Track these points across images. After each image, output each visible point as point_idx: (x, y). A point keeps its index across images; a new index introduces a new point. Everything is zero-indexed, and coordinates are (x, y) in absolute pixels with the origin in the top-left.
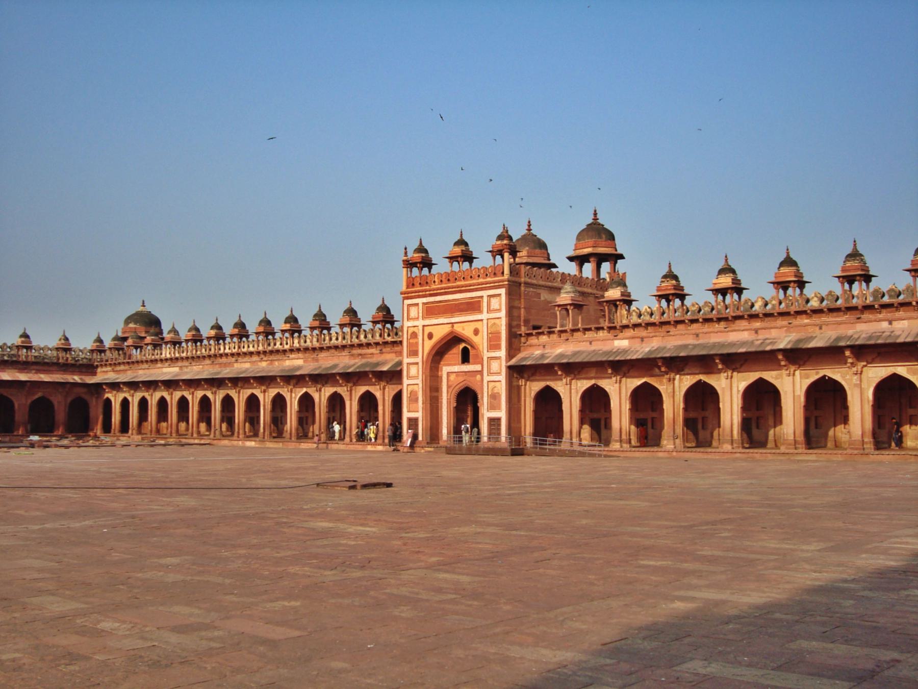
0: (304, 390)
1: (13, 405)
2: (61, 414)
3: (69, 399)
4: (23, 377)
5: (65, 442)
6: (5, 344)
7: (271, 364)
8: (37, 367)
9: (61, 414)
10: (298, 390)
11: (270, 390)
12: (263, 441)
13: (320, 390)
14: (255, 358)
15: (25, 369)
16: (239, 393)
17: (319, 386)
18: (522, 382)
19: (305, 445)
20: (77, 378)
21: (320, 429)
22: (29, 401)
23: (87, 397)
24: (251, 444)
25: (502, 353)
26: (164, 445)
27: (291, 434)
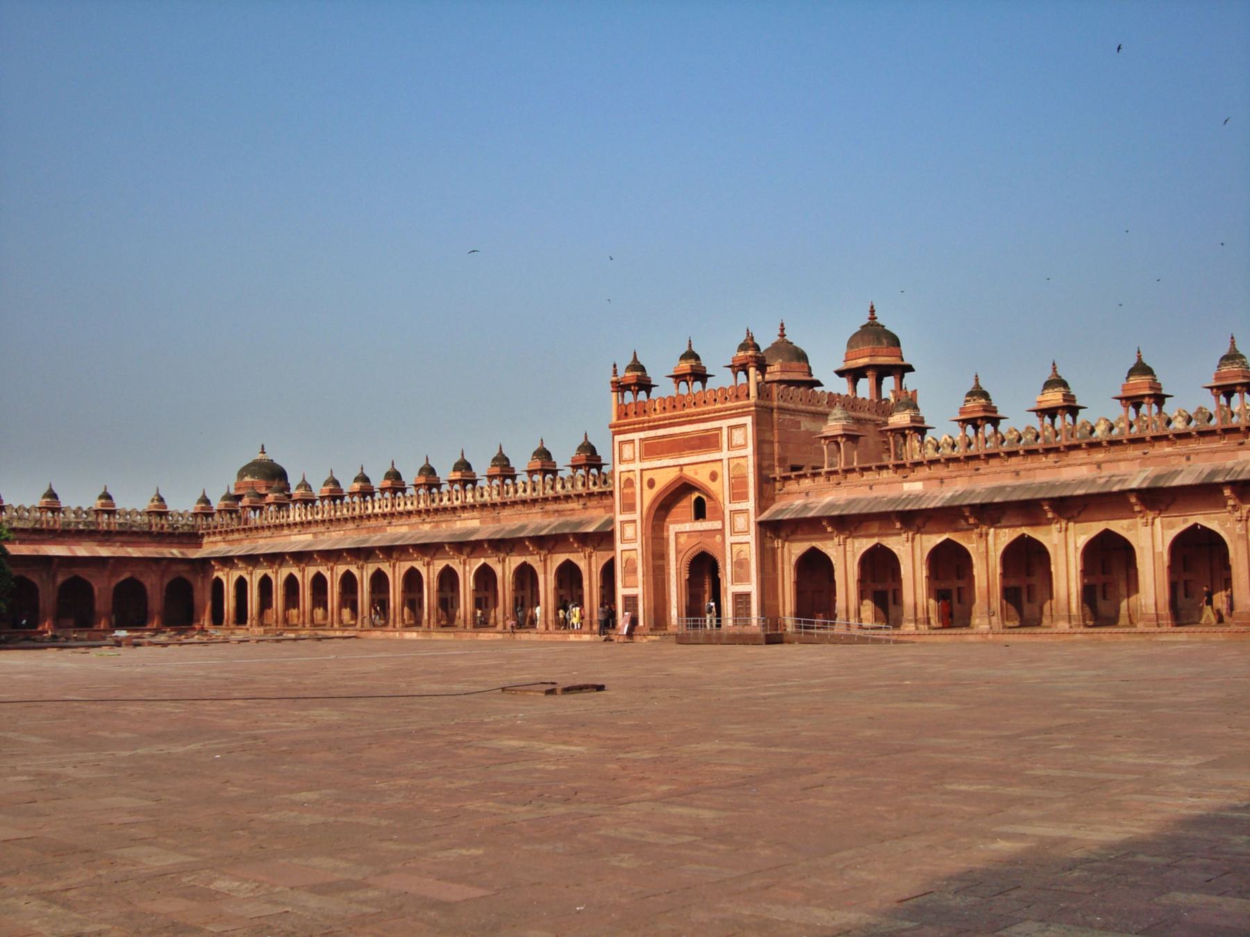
0: (482, 561)
1: (91, 589)
2: (155, 600)
3: (166, 581)
4: (104, 552)
5: (162, 638)
6: (80, 508)
7: (436, 527)
8: (125, 539)
9: (155, 600)
10: (473, 560)
11: (436, 562)
12: (428, 631)
13: (504, 561)
14: (415, 519)
15: (107, 541)
16: (394, 567)
18: (778, 543)
19: (484, 636)
20: (176, 552)
21: (504, 614)
22: (113, 585)
24: (411, 635)
25: (750, 504)
26: (295, 640)
27: (465, 621)
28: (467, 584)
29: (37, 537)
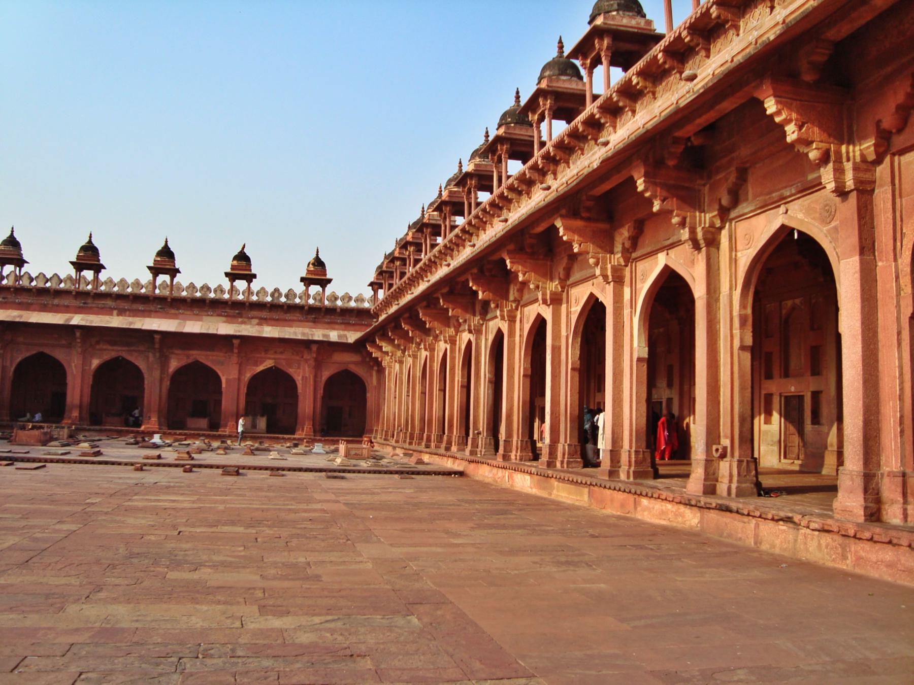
0: (662, 260)
2: (308, 402)
3: (326, 374)
5: (75, 452)
6: (263, 289)
8: (264, 314)
9: (308, 402)
10: (641, 266)
13: (712, 242)
17: (707, 218)
20: (334, 336)
22: (248, 376)
23: (360, 371)
26: (406, 473)
27: (615, 454)
28: (628, 343)
29: (141, 307)
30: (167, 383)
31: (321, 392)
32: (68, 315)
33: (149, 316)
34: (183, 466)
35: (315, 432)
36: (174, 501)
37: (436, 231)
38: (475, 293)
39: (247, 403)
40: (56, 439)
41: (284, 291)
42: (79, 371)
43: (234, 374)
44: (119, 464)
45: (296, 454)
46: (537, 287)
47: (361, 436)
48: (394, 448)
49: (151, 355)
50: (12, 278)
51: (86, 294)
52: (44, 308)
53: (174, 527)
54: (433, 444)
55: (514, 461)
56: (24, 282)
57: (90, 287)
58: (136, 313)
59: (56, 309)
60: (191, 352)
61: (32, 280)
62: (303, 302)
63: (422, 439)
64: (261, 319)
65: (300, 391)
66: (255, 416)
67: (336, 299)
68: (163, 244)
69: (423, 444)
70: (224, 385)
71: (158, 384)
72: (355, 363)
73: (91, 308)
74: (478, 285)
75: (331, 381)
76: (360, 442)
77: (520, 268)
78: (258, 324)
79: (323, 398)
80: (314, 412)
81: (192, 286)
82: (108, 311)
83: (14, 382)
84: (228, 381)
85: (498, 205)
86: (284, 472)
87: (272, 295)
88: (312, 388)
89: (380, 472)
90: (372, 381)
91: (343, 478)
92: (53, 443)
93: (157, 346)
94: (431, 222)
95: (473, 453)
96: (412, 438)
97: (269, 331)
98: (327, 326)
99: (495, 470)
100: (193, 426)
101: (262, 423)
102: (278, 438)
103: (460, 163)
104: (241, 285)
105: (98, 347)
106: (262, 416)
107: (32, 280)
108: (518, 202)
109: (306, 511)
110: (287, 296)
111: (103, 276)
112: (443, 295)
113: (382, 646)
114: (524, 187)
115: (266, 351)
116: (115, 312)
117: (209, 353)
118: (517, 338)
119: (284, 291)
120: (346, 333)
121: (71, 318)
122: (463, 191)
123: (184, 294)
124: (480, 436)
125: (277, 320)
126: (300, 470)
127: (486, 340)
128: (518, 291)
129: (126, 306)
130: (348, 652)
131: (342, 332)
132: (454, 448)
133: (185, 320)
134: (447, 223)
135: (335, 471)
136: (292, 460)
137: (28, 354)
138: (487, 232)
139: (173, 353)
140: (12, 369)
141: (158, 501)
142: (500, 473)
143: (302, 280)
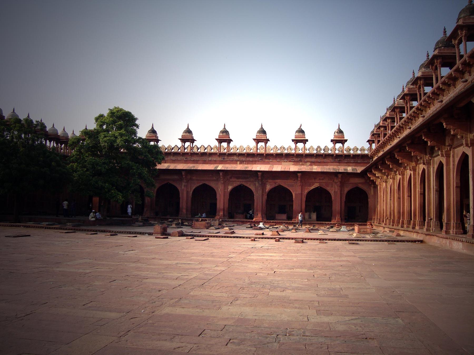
2: (337, 205)
3: (346, 190)
5: (223, 232)
6: (312, 146)
8: (313, 160)
9: (337, 205)
15: (301, 161)
22: (306, 192)
29: (251, 159)
30: (265, 197)
31: (344, 198)
32: (216, 165)
33: (255, 164)
34: (275, 238)
35: (341, 220)
36: (271, 256)
37: (402, 110)
38: (426, 142)
39: (306, 205)
40: (213, 226)
41: (322, 147)
42: (222, 192)
43: (299, 191)
44: (244, 238)
45: (333, 232)
46: (462, 137)
47: (366, 222)
48: (384, 228)
49: (257, 183)
50: (189, 148)
51: (224, 154)
52: (205, 162)
53: (272, 269)
54: (405, 226)
55: (452, 234)
56: (195, 150)
57: (225, 151)
58: (249, 162)
59: (210, 162)
60: (277, 181)
61: (198, 149)
62: (333, 153)
63: (399, 223)
64: (311, 162)
65: (333, 199)
66: (310, 212)
67: (350, 150)
68: (260, 127)
69: (400, 225)
70: (294, 197)
71: (261, 199)
72: (361, 183)
73: (227, 161)
74: (427, 138)
75: (349, 193)
76: (366, 225)
77: (452, 127)
78: (310, 165)
79: (345, 202)
80: (341, 210)
81: (276, 147)
82: (235, 162)
83: (192, 198)
84: (295, 194)
85: (437, 93)
86: (326, 241)
87: (317, 150)
88: (339, 197)
89: (377, 241)
90: (371, 192)
91: (357, 244)
92: (211, 228)
93: (260, 178)
94: (399, 105)
95: (427, 230)
96: (393, 222)
97: (316, 168)
98: (345, 164)
99: (441, 239)
100: (279, 218)
101: (314, 216)
102: (323, 224)
103: (414, 72)
104: (300, 145)
105: (231, 180)
106: (314, 212)
107: (198, 149)
108: (448, 91)
109: (338, 261)
110: (324, 150)
111: (232, 145)
112: (408, 144)
113: (383, 334)
114: (452, 82)
115: (315, 179)
116: (238, 162)
117: (286, 181)
118: (451, 166)
119: (322, 147)
120: (356, 167)
121: (217, 167)
122: (416, 87)
123: (272, 152)
124: (432, 221)
125: (320, 162)
126: (335, 240)
127: (433, 168)
128: (450, 140)
129: (244, 159)
130: (364, 336)
131: (354, 167)
132: (417, 228)
133: (273, 165)
134: (408, 105)
135: (353, 240)
136: (330, 235)
137: (198, 185)
138: (431, 109)
139: (267, 182)
140: (191, 193)
141: (264, 256)
142: (444, 241)
143: (332, 141)
